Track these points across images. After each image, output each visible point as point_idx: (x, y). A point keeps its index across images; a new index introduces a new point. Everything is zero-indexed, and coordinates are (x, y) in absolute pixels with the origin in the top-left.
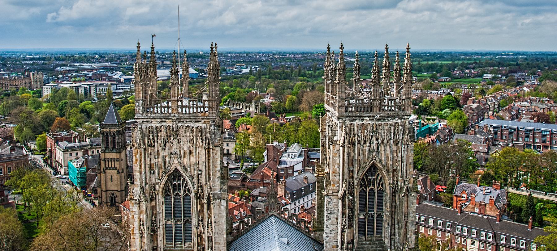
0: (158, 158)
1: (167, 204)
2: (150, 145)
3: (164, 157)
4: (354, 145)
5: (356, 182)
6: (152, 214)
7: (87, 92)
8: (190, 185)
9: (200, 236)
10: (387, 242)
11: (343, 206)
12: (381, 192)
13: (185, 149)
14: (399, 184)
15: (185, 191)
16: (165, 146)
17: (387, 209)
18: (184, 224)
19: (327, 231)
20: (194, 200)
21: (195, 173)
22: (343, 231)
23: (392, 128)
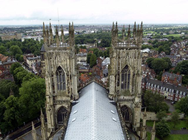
0: (53, 62)
1: (57, 78)
2: (50, 58)
3: (56, 62)
4: (120, 58)
5: (120, 71)
6: (53, 81)
7: (37, 40)
8: (64, 71)
9: (68, 88)
10: (131, 91)
11: (116, 79)
12: (129, 75)
13: (63, 59)
14: (136, 72)
15: (63, 73)
16: (55, 58)
17: (131, 80)
18: (63, 84)
19: (110, 87)
20: (66, 76)
21: (66, 67)
22: (115, 87)
23: (134, 52)
